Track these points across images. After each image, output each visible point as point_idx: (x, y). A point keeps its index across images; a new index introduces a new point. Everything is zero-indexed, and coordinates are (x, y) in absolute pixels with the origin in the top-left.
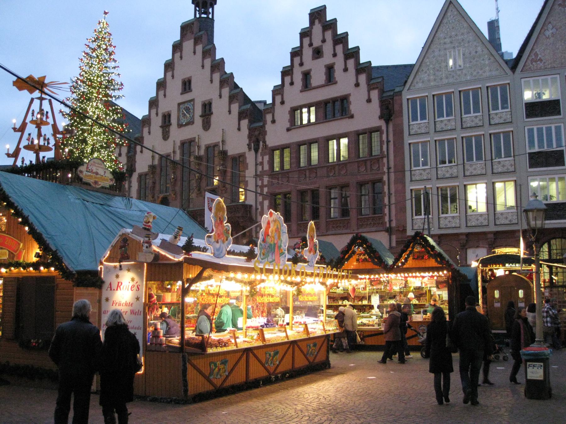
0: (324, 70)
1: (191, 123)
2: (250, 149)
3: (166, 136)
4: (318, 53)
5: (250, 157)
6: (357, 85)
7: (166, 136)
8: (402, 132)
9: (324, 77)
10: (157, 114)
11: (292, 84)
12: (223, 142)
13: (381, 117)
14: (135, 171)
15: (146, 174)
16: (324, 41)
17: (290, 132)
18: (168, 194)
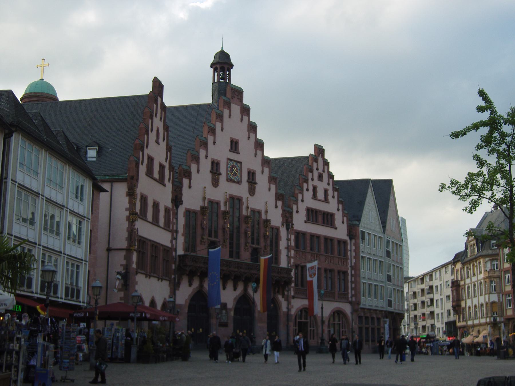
0: (323, 191)
1: (239, 182)
2: (283, 224)
3: (215, 183)
4: (320, 177)
5: (283, 232)
6: (338, 210)
7: (215, 183)
8: (359, 249)
9: (323, 196)
10: (207, 157)
11: (308, 190)
12: (266, 212)
13: (347, 235)
14: (182, 204)
15: (195, 212)
16: (324, 171)
17: (306, 224)
18: (218, 240)
